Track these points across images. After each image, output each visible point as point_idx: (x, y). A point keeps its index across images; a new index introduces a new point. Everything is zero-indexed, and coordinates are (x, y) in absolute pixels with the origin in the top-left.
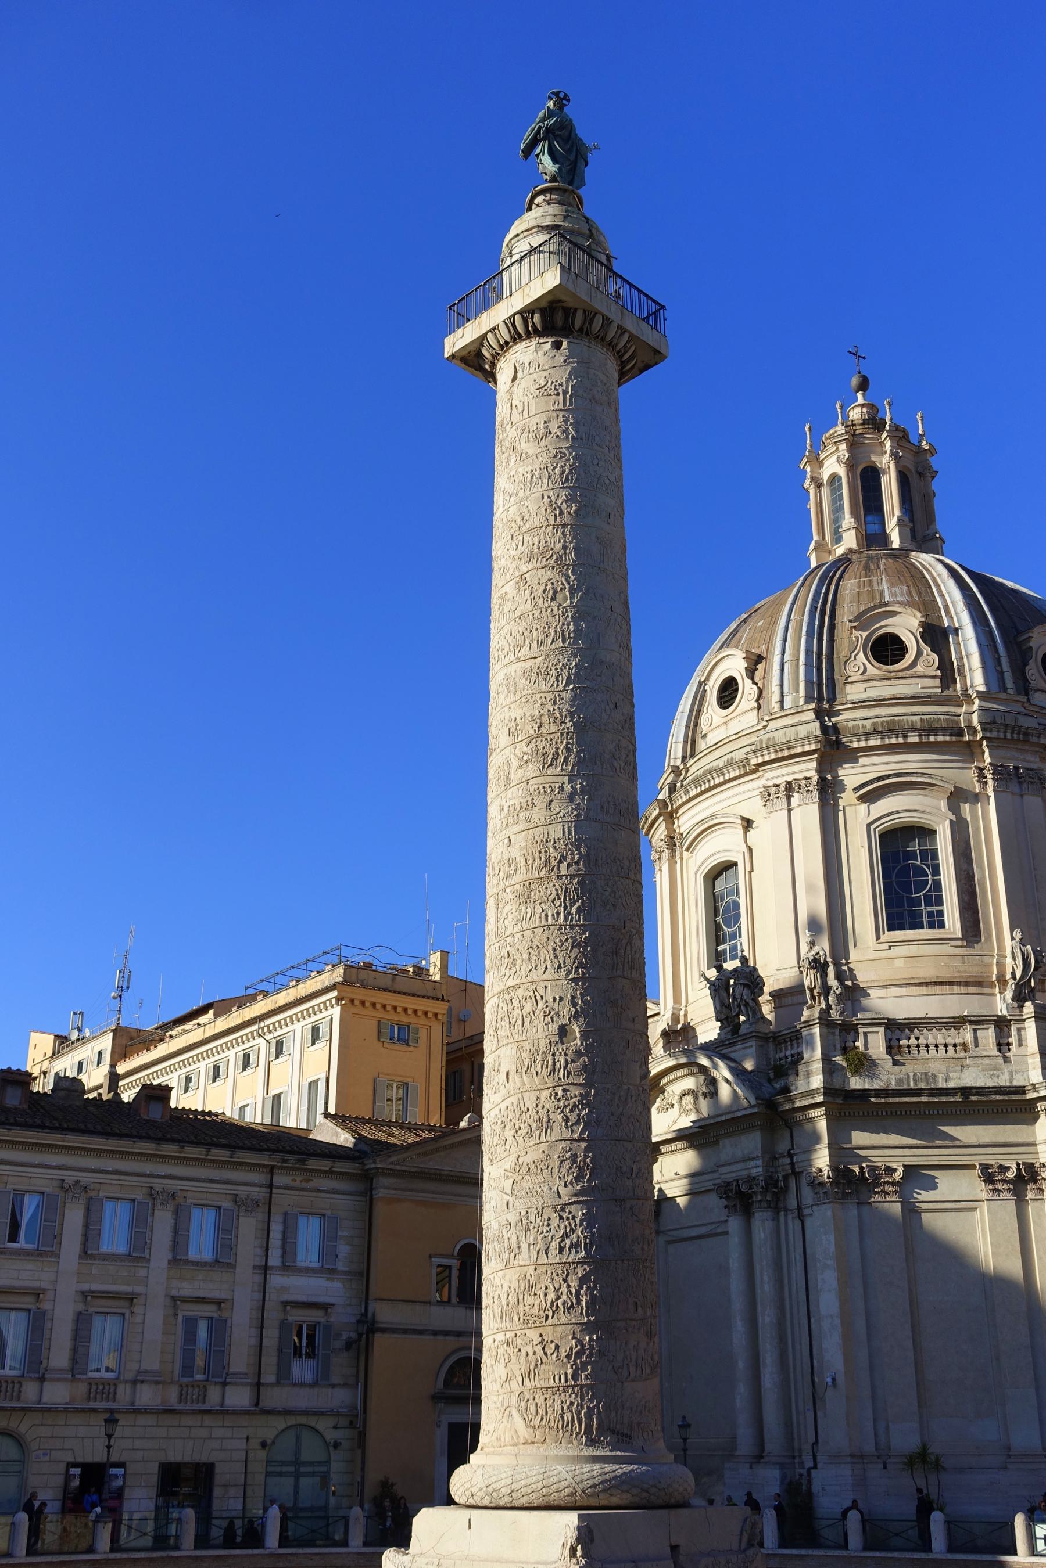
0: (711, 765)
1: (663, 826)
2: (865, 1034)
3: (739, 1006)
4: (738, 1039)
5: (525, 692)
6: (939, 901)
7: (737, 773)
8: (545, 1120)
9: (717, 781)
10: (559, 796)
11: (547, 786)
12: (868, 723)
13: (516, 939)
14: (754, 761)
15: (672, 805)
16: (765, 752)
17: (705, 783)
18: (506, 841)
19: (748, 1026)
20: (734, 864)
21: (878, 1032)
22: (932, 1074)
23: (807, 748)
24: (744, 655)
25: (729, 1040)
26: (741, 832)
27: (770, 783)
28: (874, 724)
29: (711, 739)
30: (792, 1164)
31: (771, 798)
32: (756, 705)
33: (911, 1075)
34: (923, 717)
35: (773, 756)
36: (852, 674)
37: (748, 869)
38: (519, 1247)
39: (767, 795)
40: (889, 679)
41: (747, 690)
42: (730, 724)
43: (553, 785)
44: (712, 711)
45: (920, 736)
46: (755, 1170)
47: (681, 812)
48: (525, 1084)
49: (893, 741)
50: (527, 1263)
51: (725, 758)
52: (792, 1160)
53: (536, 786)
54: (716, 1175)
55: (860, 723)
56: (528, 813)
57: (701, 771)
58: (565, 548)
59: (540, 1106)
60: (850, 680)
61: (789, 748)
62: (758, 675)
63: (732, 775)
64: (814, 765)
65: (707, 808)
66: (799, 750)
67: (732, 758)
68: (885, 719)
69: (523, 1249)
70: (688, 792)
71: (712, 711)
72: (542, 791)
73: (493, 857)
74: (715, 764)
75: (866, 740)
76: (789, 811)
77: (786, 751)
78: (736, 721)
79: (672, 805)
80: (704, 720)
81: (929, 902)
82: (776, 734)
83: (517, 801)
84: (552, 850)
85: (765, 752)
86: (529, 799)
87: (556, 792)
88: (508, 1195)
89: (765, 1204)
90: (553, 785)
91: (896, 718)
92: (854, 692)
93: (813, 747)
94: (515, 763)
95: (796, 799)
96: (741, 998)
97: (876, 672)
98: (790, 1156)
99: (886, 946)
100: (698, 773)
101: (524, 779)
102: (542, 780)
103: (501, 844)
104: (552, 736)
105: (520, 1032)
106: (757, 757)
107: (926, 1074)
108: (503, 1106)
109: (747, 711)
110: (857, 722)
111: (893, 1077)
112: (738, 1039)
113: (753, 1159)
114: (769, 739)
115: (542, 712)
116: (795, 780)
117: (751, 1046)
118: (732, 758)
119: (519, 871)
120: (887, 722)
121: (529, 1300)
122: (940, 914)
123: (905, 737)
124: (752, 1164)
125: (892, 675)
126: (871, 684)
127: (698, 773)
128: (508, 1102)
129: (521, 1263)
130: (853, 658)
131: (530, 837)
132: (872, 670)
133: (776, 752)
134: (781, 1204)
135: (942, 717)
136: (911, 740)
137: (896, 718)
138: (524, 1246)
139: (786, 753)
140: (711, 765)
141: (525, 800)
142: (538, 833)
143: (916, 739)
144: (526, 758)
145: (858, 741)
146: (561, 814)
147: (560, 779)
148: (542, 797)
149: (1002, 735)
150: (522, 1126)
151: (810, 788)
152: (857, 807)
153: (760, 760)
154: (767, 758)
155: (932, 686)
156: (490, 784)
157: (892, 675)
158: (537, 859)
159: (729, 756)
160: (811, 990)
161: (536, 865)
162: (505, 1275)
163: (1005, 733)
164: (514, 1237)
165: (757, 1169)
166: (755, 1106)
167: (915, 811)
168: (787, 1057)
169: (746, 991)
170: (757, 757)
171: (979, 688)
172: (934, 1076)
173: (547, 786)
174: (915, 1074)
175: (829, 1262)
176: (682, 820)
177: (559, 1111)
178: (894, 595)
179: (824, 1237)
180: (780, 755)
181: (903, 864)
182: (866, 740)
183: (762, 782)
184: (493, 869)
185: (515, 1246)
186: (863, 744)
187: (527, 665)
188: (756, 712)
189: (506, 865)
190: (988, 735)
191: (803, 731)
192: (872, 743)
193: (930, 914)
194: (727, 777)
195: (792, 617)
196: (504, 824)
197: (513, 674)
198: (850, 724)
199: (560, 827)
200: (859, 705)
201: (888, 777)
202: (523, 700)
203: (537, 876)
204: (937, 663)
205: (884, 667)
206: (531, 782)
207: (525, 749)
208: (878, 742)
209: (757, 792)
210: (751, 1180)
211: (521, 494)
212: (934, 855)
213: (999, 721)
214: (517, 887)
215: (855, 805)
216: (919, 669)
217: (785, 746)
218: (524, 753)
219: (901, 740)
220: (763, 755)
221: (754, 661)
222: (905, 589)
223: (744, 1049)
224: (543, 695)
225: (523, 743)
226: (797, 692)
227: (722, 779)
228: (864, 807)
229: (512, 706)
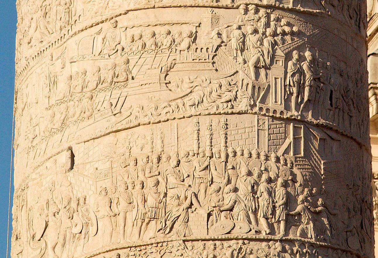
10: (191, 55)
11: (161, 31)
18: (65, 157)
43: (175, 30)
53: (136, 32)
56: (116, 93)
72: (149, 42)
73: (31, 196)
83: (89, 66)
84: (172, 180)
86: (120, 59)
87: (184, 45)
90: (175, 30)
101: (108, 14)
103: (49, 164)
119: (92, 230)
131: (121, 151)
141: (110, 62)
142: (140, 142)
146: (195, 97)
147: (195, 15)
148: (148, 57)
156: (21, 26)
158: (137, 199)
161: (131, 216)
173: (161, 31)
184: (30, 223)
189: (63, 215)
196: (59, 117)
199: (189, 126)
203: (135, 240)
206: (123, 21)
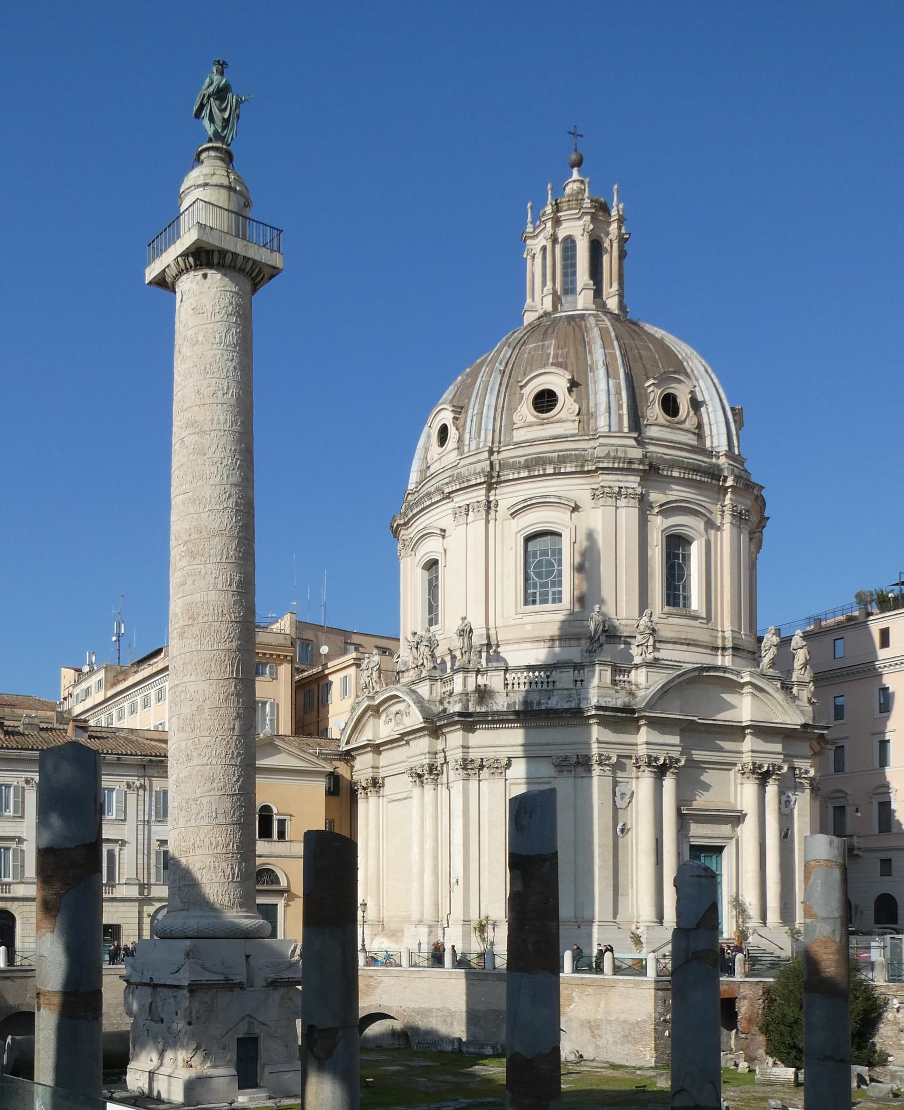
6: (560, 584)
12: (522, 460)
34: (561, 453)
40: (542, 424)
41: (453, 433)
45: (555, 468)
49: (536, 473)
58: (205, 419)
60: (515, 426)
62: (460, 422)
75: (519, 473)
81: (554, 584)
91: (542, 455)
97: (535, 420)
110: (515, 459)
120: (535, 458)
122: (560, 592)
123: (545, 470)
125: (545, 421)
126: (530, 429)
132: (531, 419)
135: (573, 453)
136: (548, 472)
137: (542, 455)
143: (552, 471)
149: (611, 465)
155: (571, 428)
163: (614, 463)
171: (602, 430)
182: (519, 473)
190: (601, 465)
192: (522, 475)
193: (554, 593)
198: (511, 461)
200: (519, 445)
211: (183, 384)
212: (560, 552)
213: (612, 454)
216: (563, 415)
219: (541, 472)
221: (459, 410)
226: (479, 437)
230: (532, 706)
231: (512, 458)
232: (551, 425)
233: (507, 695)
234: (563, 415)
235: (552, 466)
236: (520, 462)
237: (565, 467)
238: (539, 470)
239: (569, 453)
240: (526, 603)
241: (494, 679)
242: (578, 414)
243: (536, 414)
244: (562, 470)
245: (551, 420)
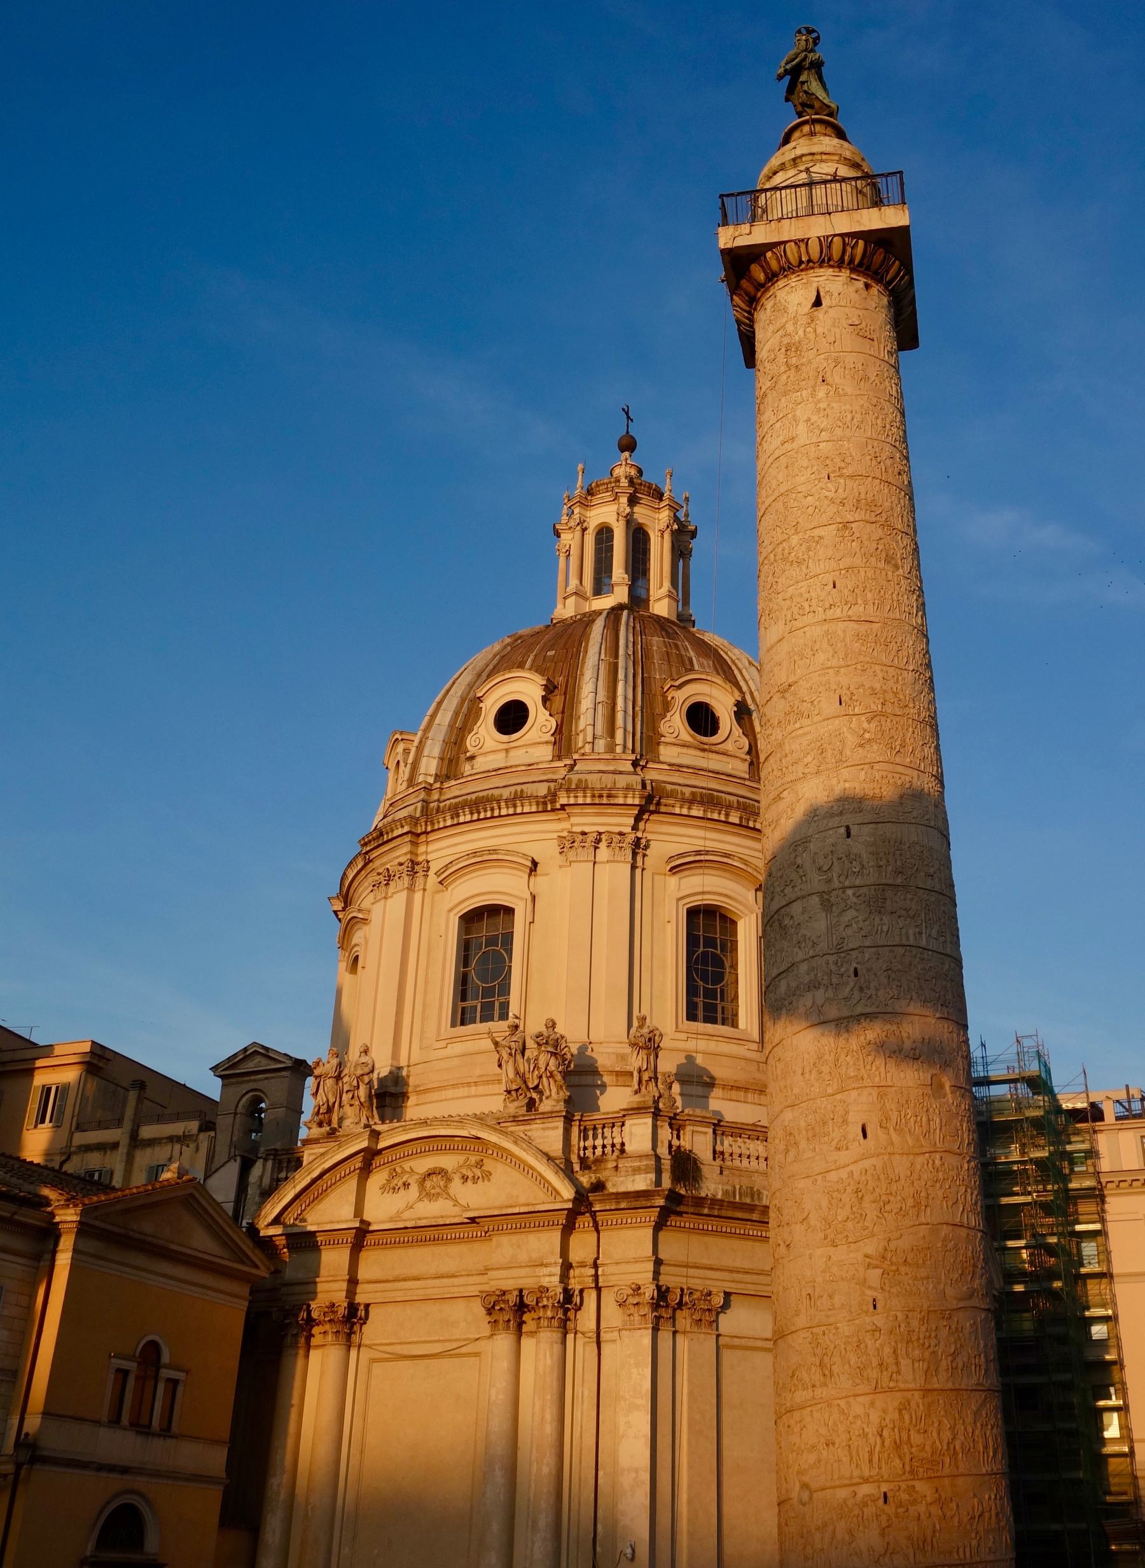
0: (490, 792)
1: (407, 848)
2: (693, 1132)
3: (541, 1077)
4: (537, 1117)
5: (861, 658)
7: (534, 809)
8: (923, 1194)
9: (504, 812)
12: (687, 791)
13: (867, 955)
14: (564, 801)
15: (426, 825)
16: (580, 794)
17: (486, 811)
18: (843, 830)
19: (553, 1103)
20: (510, 911)
21: (706, 1133)
22: (758, 1190)
23: (630, 801)
24: (544, 682)
25: (524, 1116)
26: (526, 876)
27: (578, 829)
28: (693, 793)
29: (481, 764)
30: (596, 1276)
31: (575, 844)
32: (553, 739)
33: (738, 1187)
34: (741, 800)
35: (588, 801)
36: (667, 735)
37: (529, 919)
38: (897, 1364)
39: (569, 843)
40: (704, 750)
41: (541, 722)
42: (512, 753)
44: (485, 733)
45: (741, 818)
46: (547, 1279)
47: (432, 837)
48: (892, 1143)
49: (715, 816)
50: (912, 1386)
51: (513, 789)
52: (597, 1271)
53: (884, 774)
54: (484, 1279)
55: (679, 788)
57: (474, 796)
59: (915, 1176)
61: (609, 796)
63: (526, 809)
64: (631, 821)
65: (729, 843)
66: (621, 801)
67: (522, 791)
68: (704, 791)
69: (903, 1368)
70: (458, 816)
71: (485, 733)
74: (496, 792)
76: (595, 863)
77: (605, 799)
78: (522, 751)
79: (426, 825)
80: (470, 742)
82: (590, 777)
85: (580, 794)
88: (875, 1289)
89: (555, 1323)
91: (715, 793)
92: (667, 753)
93: (637, 802)
94: (851, 740)
95: (604, 852)
96: (546, 1069)
97: (689, 739)
98: (596, 1266)
99: (683, 1036)
100: (469, 797)
102: (890, 767)
104: (898, 719)
105: (883, 1075)
106: (569, 797)
107: (752, 1188)
108: (856, 1169)
109: (539, 743)
111: (720, 1187)
112: (537, 1117)
113: (546, 1266)
114: (580, 781)
115: (884, 688)
116: (608, 832)
117: (557, 1128)
118: (522, 791)
121: (916, 1438)
123: (727, 815)
124: (546, 1271)
125: (706, 747)
126: (685, 750)
127: (469, 797)
128: (867, 1164)
129: (902, 1386)
130: (668, 718)
133: (593, 796)
134: (570, 1325)
138: (904, 1362)
139: (605, 801)
140: (490, 792)
143: (737, 821)
144: (867, 736)
145: (681, 807)
150: (892, 1198)
151: (624, 845)
152: (667, 877)
153: (572, 801)
154: (580, 801)
155: (740, 768)
157: (706, 747)
159: (519, 788)
160: (640, 1071)
162: (872, 1404)
164: (887, 1350)
165: (551, 1278)
166: (569, 1200)
167: (726, 896)
168: (595, 1147)
169: (553, 1062)
170: (569, 797)
172: (759, 1193)
174: (741, 1187)
175: (639, 1402)
176: (431, 848)
177: (938, 1185)
178: (702, 665)
179: (634, 1371)
180: (597, 801)
181: (701, 949)
182: (689, 808)
183: (565, 825)
185: (891, 1360)
186: (685, 811)
187: (864, 628)
188: (550, 747)
191: (622, 781)
192: (694, 813)
194: (519, 810)
195: (603, 657)
197: (840, 632)
198: (669, 787)
200: (677, 767)
201: (707, 853)
202: (859, 666)
203: (891, 882)
204: (747, 748)
205: (699, 737)
207: (865, 725)
208: (701, 814)
209: (555, 835)
210: (544, 1290)
214: (864, 890)
215: (665, 875)
217: (605, 793)
218: (865, 731)
219: (723, 818)
220: (576, 797)
222: (711, 663)
223: (543, 1129)
224: (885, 668)
225: (863, 718)
227: (511, 811)
228: (673, 881)
229: (843, 670)
230: (760, 1199)
231: (670, 783)
232: (714, 756)
233: (721, 1173)
234: (729, 746)
235: (738, 814)
236: (683, 794)
237: (755, 821)
238: (720, 814)
239: (751, 802)
240: (453, 1025)
241: (697, 1138)
242: (749, 753)
243: (693, 733)
244: (751, 824)
245: (713, 748)
